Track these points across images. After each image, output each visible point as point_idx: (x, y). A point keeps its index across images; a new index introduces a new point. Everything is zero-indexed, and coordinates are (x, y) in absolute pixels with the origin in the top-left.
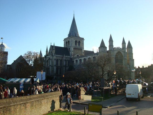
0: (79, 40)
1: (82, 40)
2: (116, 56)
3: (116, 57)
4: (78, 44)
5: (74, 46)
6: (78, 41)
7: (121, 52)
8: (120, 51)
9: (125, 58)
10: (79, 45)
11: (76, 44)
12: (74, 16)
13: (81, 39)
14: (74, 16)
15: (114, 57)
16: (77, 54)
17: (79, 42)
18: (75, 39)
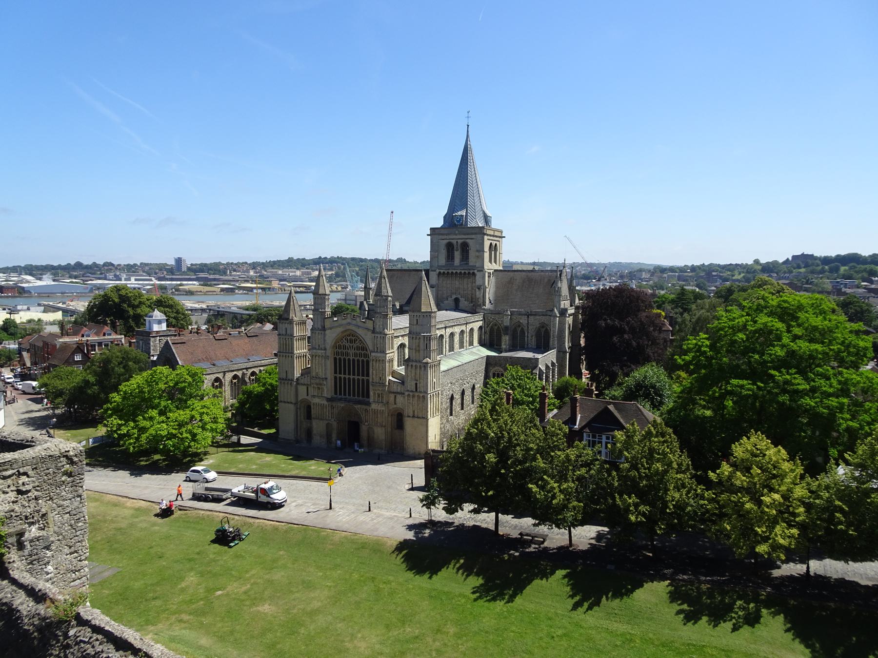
1: (473, 236)
2: (335, 346)
3: (338, 353)
4: (457, 255)
5: (440, 267)
6: (460, 241)
7: (360, 332)
8: (354, 328)
9: (373, 354)
11: (450, 257)
12: (468, 136)
13: (472, 234)
14: (468, 136)
15: (329, 352)
16: (454, 297)
17: (465, 247)
18: (445, 237)
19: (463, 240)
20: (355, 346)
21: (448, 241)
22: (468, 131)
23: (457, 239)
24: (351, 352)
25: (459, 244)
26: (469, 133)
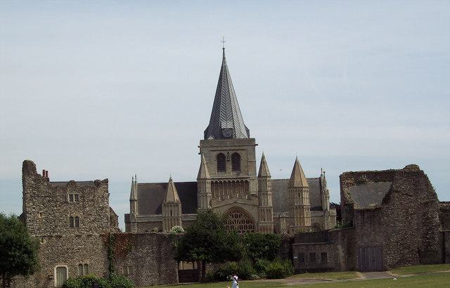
0: (232, 148)
4: (229, 166)
6: (231, 153)
7: (245, 208)
8: (240, 206)
10: (236, 167)
11: (221, 167)
12: (224, 58)
14: (224, 58)
17: (236, 159)
18: (216, 149)
19: (234, 152)
20: (240, 219)
21: (218, 152)
22: (224, 54)
23: (228, 151)
24: (236, 226)
25: (230, 154)
26: (226, 56)
